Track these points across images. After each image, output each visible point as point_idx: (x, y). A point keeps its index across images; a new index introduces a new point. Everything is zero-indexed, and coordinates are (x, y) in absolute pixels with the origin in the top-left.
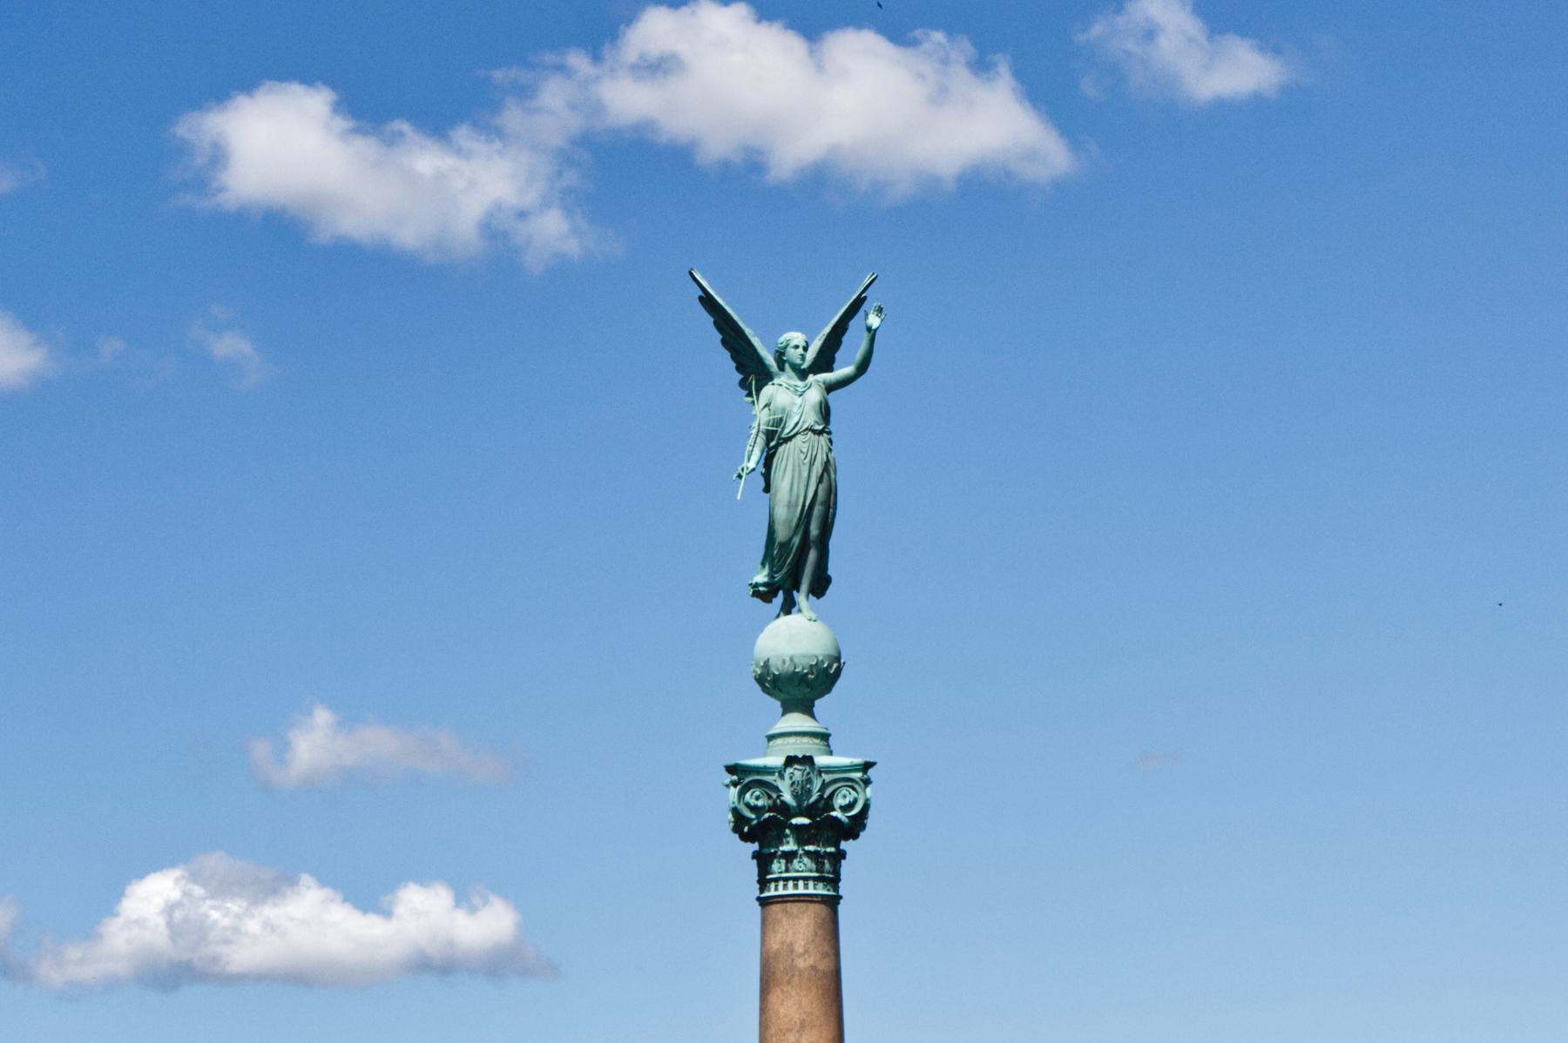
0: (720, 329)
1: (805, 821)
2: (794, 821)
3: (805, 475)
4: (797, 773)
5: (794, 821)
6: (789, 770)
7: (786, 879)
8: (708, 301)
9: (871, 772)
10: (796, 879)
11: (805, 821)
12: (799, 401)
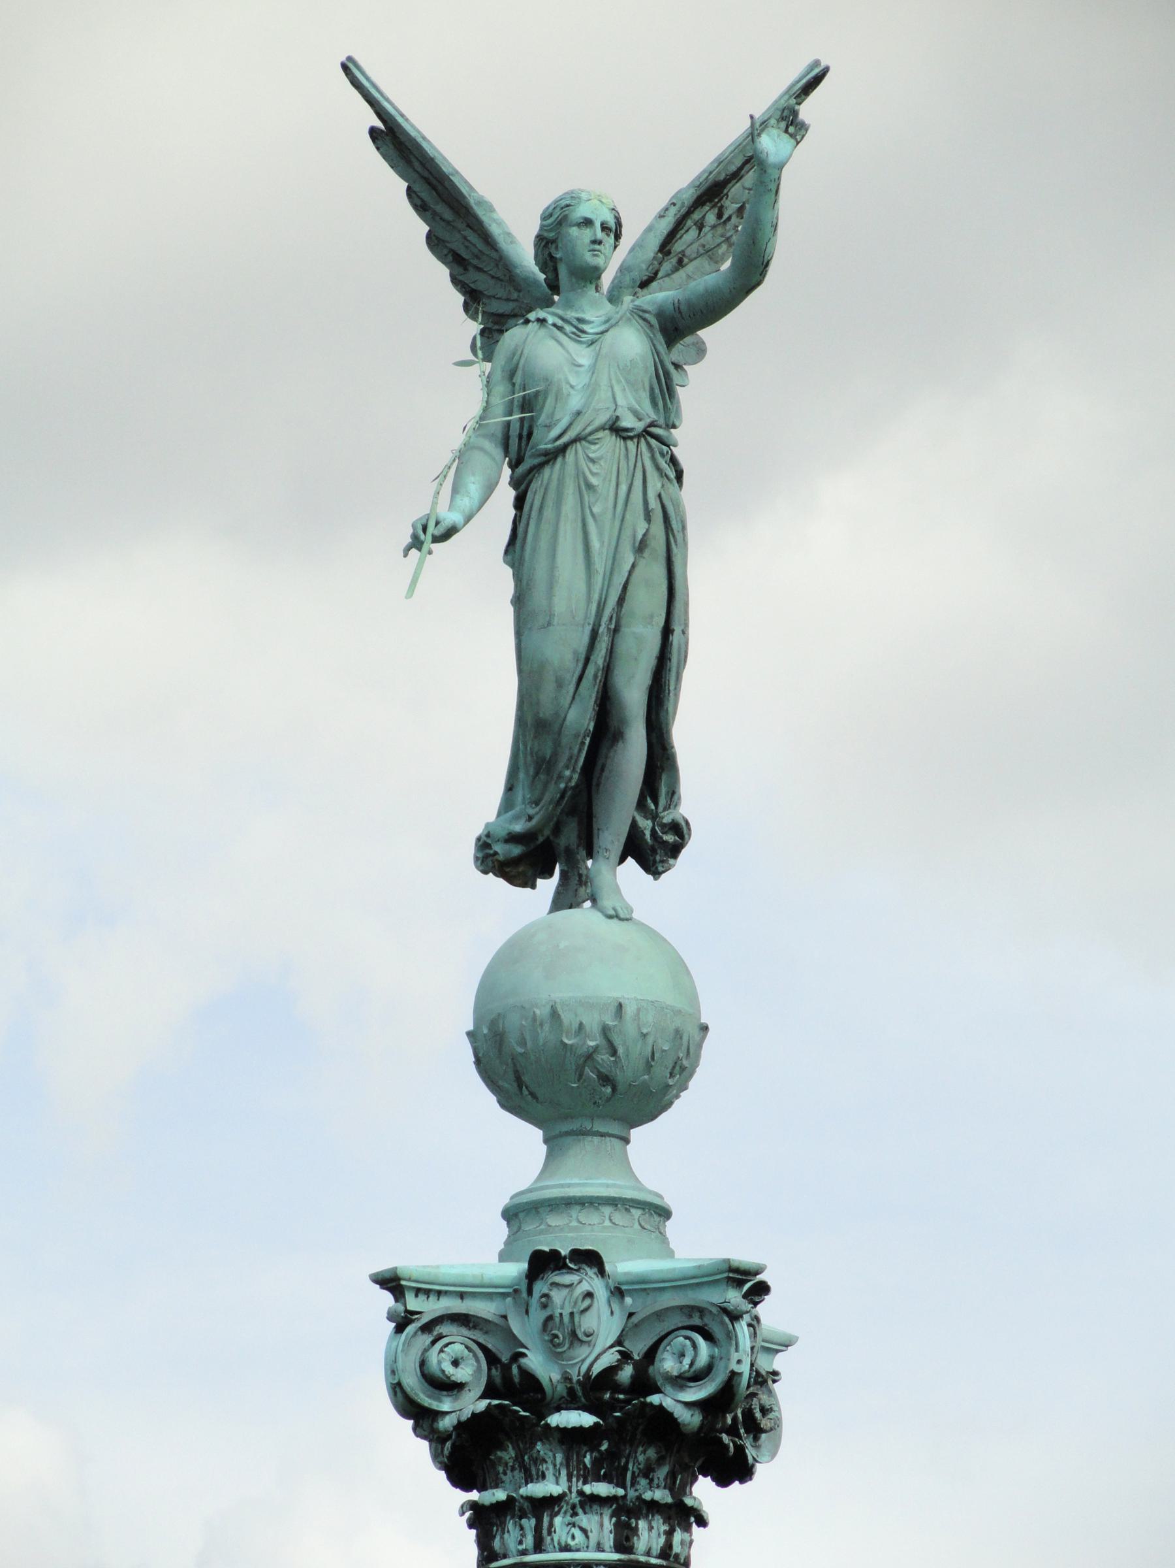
0: (421, 207)
2: (558, 1419)
6: (540, 1287)
8: (394, 141)
12: (584, 356)
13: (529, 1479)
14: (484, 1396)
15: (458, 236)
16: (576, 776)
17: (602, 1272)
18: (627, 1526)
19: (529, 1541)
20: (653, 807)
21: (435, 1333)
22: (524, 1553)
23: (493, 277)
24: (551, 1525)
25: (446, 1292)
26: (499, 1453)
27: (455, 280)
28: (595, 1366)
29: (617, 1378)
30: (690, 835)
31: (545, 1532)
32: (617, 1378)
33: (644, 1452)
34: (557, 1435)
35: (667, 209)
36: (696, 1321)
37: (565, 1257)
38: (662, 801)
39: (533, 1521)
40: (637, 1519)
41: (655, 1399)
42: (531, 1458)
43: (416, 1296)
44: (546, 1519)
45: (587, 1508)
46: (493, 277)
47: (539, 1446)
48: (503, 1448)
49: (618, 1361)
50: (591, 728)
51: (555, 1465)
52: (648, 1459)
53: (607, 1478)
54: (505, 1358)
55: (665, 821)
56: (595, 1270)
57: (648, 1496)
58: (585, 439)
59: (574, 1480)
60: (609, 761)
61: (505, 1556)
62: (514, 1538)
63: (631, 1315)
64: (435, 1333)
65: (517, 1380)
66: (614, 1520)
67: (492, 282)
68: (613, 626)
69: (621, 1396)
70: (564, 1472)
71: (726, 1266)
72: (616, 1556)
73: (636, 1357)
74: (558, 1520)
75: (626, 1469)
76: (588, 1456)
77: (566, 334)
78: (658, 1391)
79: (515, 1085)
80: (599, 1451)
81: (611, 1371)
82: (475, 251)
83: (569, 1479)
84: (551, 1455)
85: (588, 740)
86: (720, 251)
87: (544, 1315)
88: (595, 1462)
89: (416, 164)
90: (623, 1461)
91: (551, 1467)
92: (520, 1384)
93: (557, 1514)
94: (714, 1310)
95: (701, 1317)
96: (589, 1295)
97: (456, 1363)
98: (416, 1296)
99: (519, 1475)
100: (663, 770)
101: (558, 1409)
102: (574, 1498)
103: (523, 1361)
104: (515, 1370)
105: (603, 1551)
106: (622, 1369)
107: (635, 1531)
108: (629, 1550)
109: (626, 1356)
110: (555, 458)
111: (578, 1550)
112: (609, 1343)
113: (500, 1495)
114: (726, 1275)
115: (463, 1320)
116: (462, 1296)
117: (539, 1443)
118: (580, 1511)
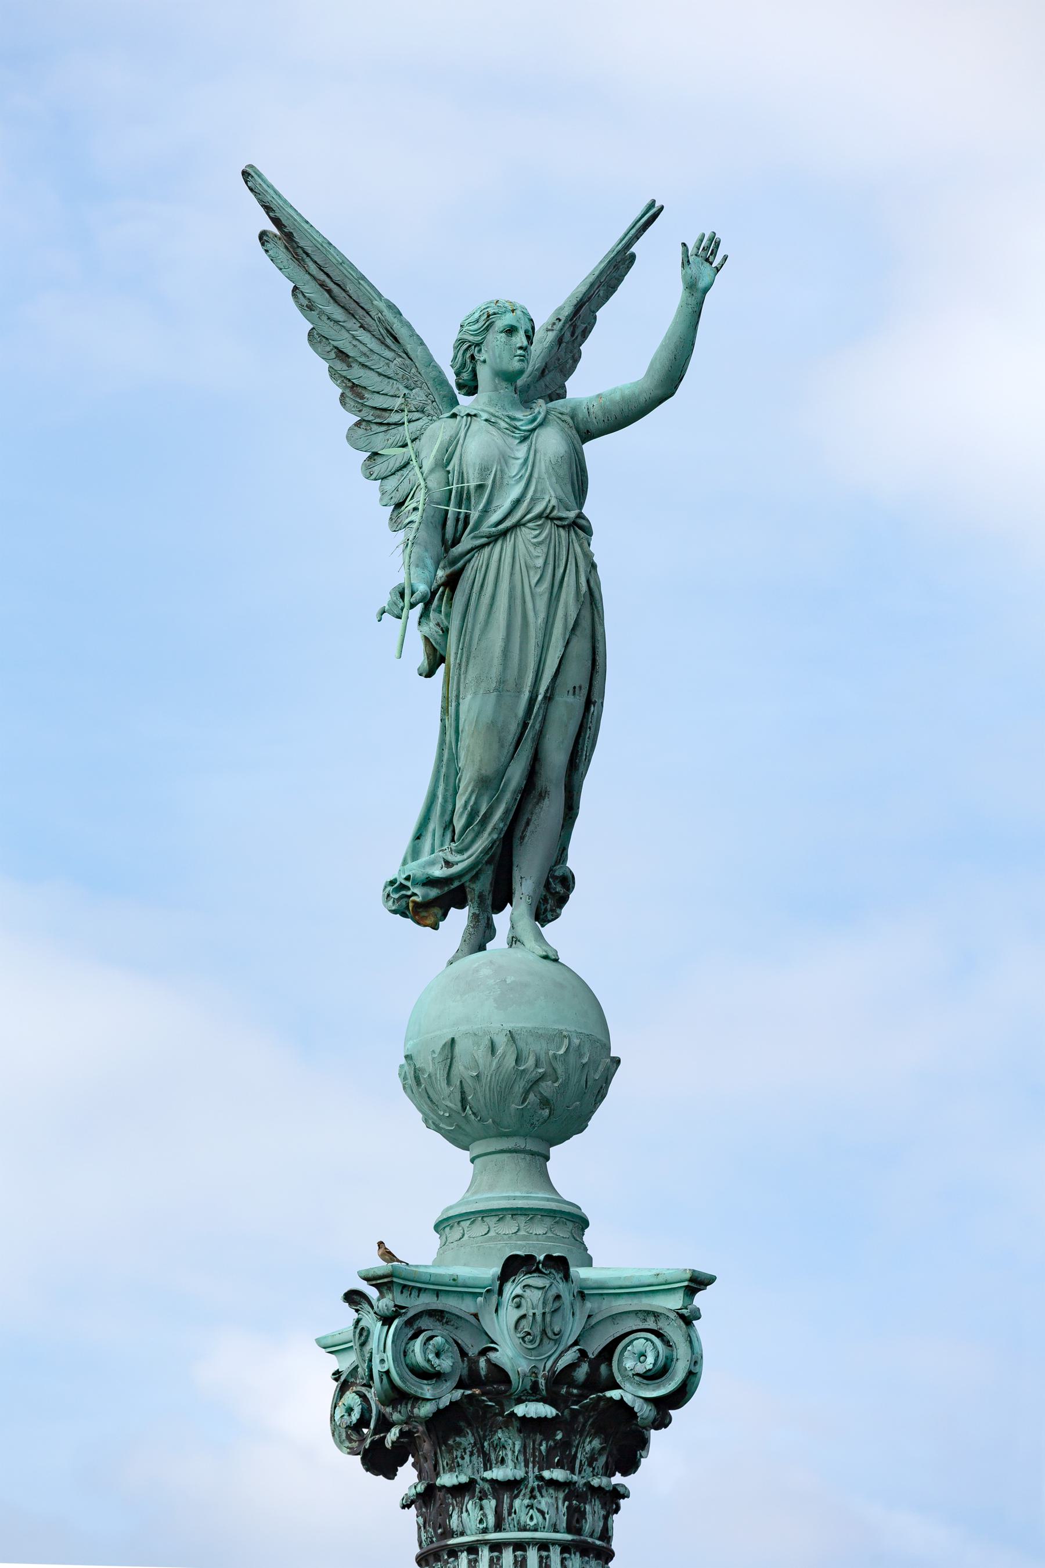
0: (308, 308)
1: (546, 1410)
2: (520, 1410)
3: (536, 621)
4: (529, 1291)
5: (520, 1410)
6: (511, 1289)
7: (496, 1547)
9: (700, 1299)
10: (519, 1546)
11: (546, 1410)
12: (521, 452)
13: (487, 1465)
14: (457, 1387)
15: (346, 335)
17: (567, 1277)
18: (577, 1509)
19: (491, 1520)
21: (415, 1327)
22: (485, 1531)
23: (380, 374)
24: (511, 1506)
25: (426, 1289)
26: (458, 1439)
27: (333, 373)
28: (560, 1362)
29: (575, 1374)
31: (505, 1512)
32: (575, 1374)
33: (590, 1442)
34: (516, 1424)
35: (554, 324)
36: (651, 1324)
37: (539, 1262)
39: (493, 1502)
40: (585, 1504)
41: (615, 1394)
42: (491, 1444)
43: (402, 1292)
44: (506, 1500)
45: (544, 1491)
46: (380, 374)
47: (500, 1434)
48: (460, 1432)
49: (579, 1358)
51: (514, 1452)
52: (593, 1449)
53: (560, 1465)
54: (472, 1352)
55: (557, 874)
56: (561, 1275)
57: (595, 1482)
58: (524, 525)
59: (531, 1465)
60: (534, 817)
61: (462, 1534)
62: (470, 1520)
63: (589, 1316)
64: (415, 1327)
65: (483, 1373)
66: (567, 1503)
67: (379, 379)
69: (575, 1391)
70: (521, 1458)
71: (688, 1276)
72: (569, 1537)
73: (591, 1356)
74: (517, 1503)
75: (575, 1456)
76: (544, 1445)
77: (499, 429)
78: (617, 1386)
79: (459, 1104)
80: (554, 1440)
81: (572, 1367)
82: (364, 349)
83: (526, 1466)
84: (512, 1442)
86: (568, 366)
87: (516, 1314)
88: (549, 1450)
89: (313, 268)
90: (574, 1450)
91: (510, 1453)
92: (486, 1376)
93: (517, 1496)
94: (672, 1315)
95: (656, 1321)
96: (558, 1297)
97: (438, 1355)
98: (402, 1292)
99: (478, 1461)
101: (519, 1401)
102: (532, 1483)
103: (492, 1355)
104: (482, 1363)
105: (558, 1532)
106: (579, 1366)
107: (583, 1514)
108: (579, 1531)
109: (583, 1353)
110: (496, 541)
111: (536, 1530)
112: (570, 1342)
113: (463, 1479)
114: (686, 1283)
115: (438, 1315)
116: (437, 1293)
117: (500, 1431)
118: (538, 1494)
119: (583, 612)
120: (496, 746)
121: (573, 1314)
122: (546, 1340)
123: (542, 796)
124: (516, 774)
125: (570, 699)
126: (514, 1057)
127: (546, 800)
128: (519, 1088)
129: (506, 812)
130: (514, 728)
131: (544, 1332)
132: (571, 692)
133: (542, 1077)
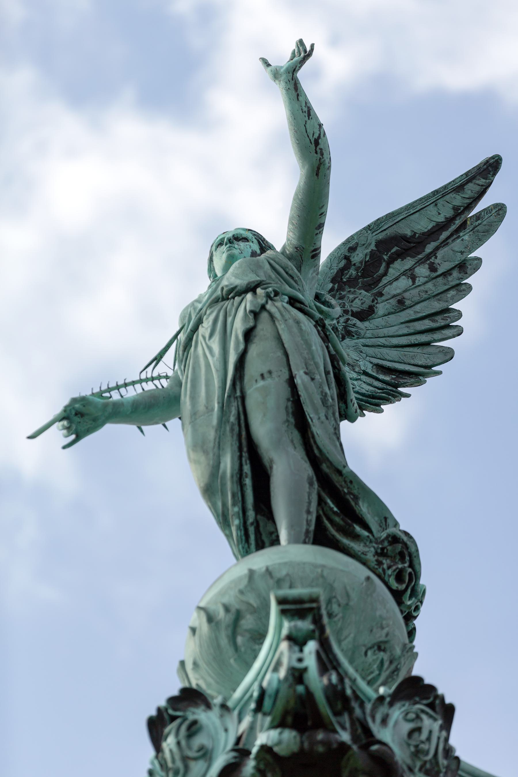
16: (251, 514)
20: (366, 534)
30: (414, 542)
37: (166, 709)
38: (374, 527)
49: (235, 757)
50: (247, 468)
56: (203, 707)
68: (238, 394)
85: (248, 482)
100: (356, 498)
106: (245, 765)
119: (260, 327)
120: (203, 459)
121: (226, 730)
122: (192, 764)
123: (271, 468)
124: (228, 463)
125: (261, 383)
126: (204, 619)
127: (275, 467)
128: (224, 641)
129: (234, 495)
130: (211, 434)
131: (185, 759)
132: (259, 378)
133: (238, 616)
